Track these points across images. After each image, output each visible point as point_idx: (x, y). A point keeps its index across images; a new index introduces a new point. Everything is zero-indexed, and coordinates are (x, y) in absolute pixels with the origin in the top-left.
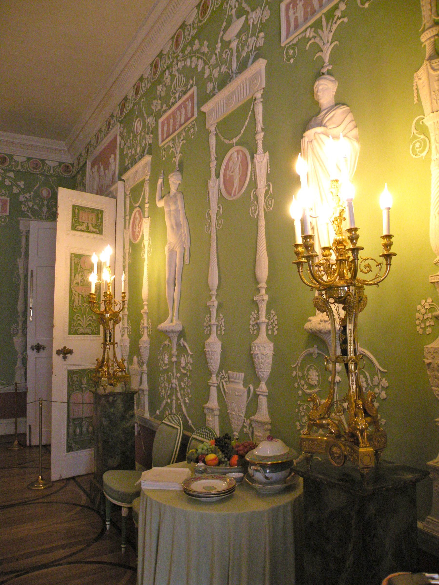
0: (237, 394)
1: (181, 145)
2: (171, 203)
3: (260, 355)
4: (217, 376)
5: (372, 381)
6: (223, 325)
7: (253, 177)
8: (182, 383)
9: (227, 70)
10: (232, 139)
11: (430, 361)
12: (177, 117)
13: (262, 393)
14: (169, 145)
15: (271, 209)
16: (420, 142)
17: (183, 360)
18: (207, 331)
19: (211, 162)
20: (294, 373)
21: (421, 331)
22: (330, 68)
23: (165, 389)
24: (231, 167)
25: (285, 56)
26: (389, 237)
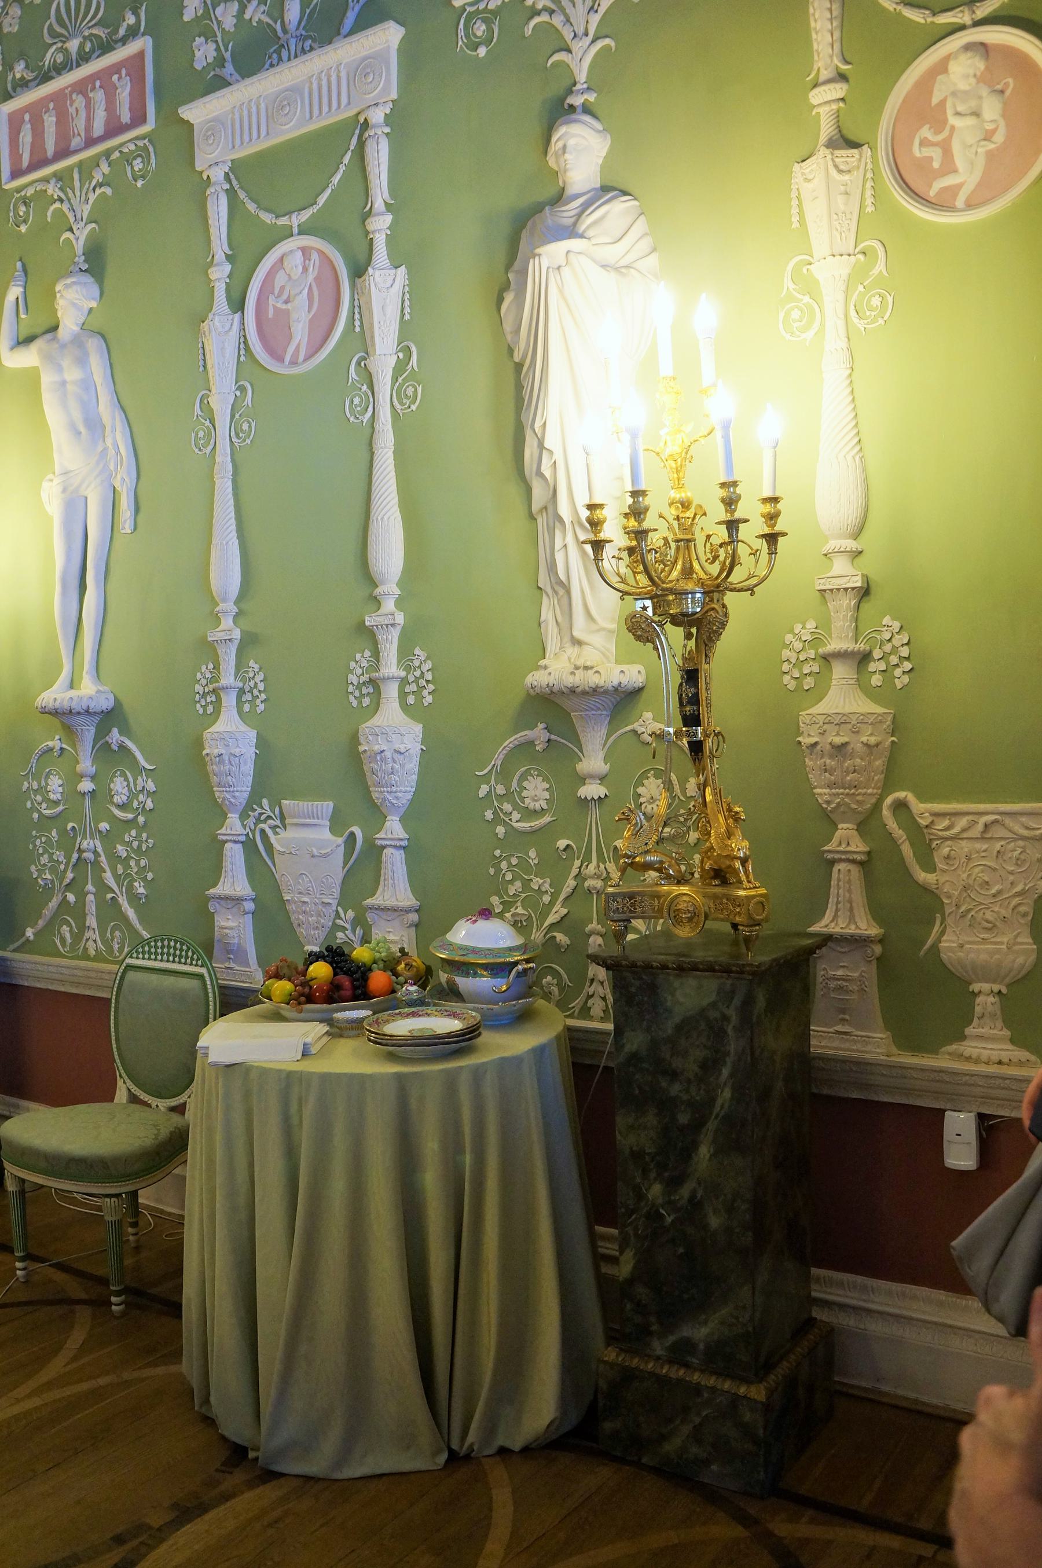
0: (315, 852)
1: (92, 197)
2: (66, 363)
3: (388, 754)
4: (244, 816)
5: (684, 790)
6: (261, 686)
7: (357, 323)
8: (119, 847)
9: (266, 19)
10: (289, 213)
11: (813, 740)
12: (72, 110)
13: (393, 843)
14: (46, 191)
15: (414, 407)
16: (801, 310)
17: (119, 786)
18: (204, 707)
19: (211, 264)
20: (484, 789)
21: (792, 685)
22: (591, 97)
23: (53, 870)
24: (282, 288)
25: (461, 33)
26: (775, 500)
